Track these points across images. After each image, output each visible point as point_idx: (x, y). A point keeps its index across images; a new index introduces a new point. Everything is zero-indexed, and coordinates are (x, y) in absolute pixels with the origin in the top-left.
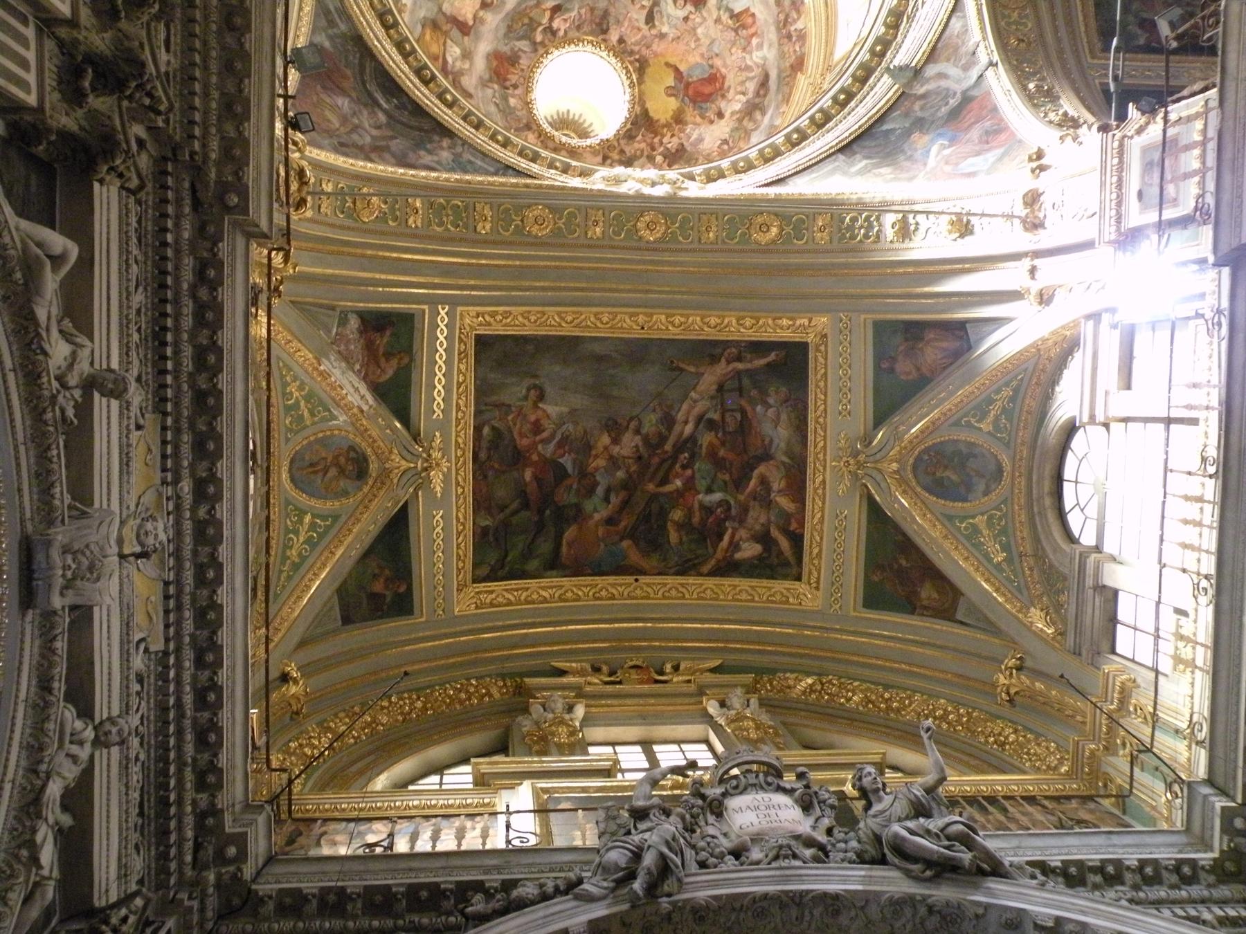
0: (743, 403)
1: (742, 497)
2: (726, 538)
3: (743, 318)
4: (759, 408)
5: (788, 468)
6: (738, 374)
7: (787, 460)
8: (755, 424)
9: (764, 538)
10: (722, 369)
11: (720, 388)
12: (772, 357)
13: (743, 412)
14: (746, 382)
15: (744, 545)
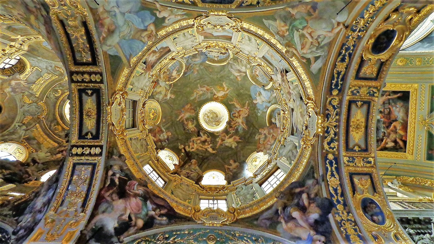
0: (390, 107)
1: (388, 131)
2: (384, 141)
3: (392, 85)
4: (394, 108)
5: (402, 124)
6: (389, 100)
7: (402, 121)
8: (393, 112)
9: (395, 142)
10: (385, 98)
11: (384, 103)
12: (399, 95)
13: (390, 109)
14: (391, 101)
15: (389, 143)
